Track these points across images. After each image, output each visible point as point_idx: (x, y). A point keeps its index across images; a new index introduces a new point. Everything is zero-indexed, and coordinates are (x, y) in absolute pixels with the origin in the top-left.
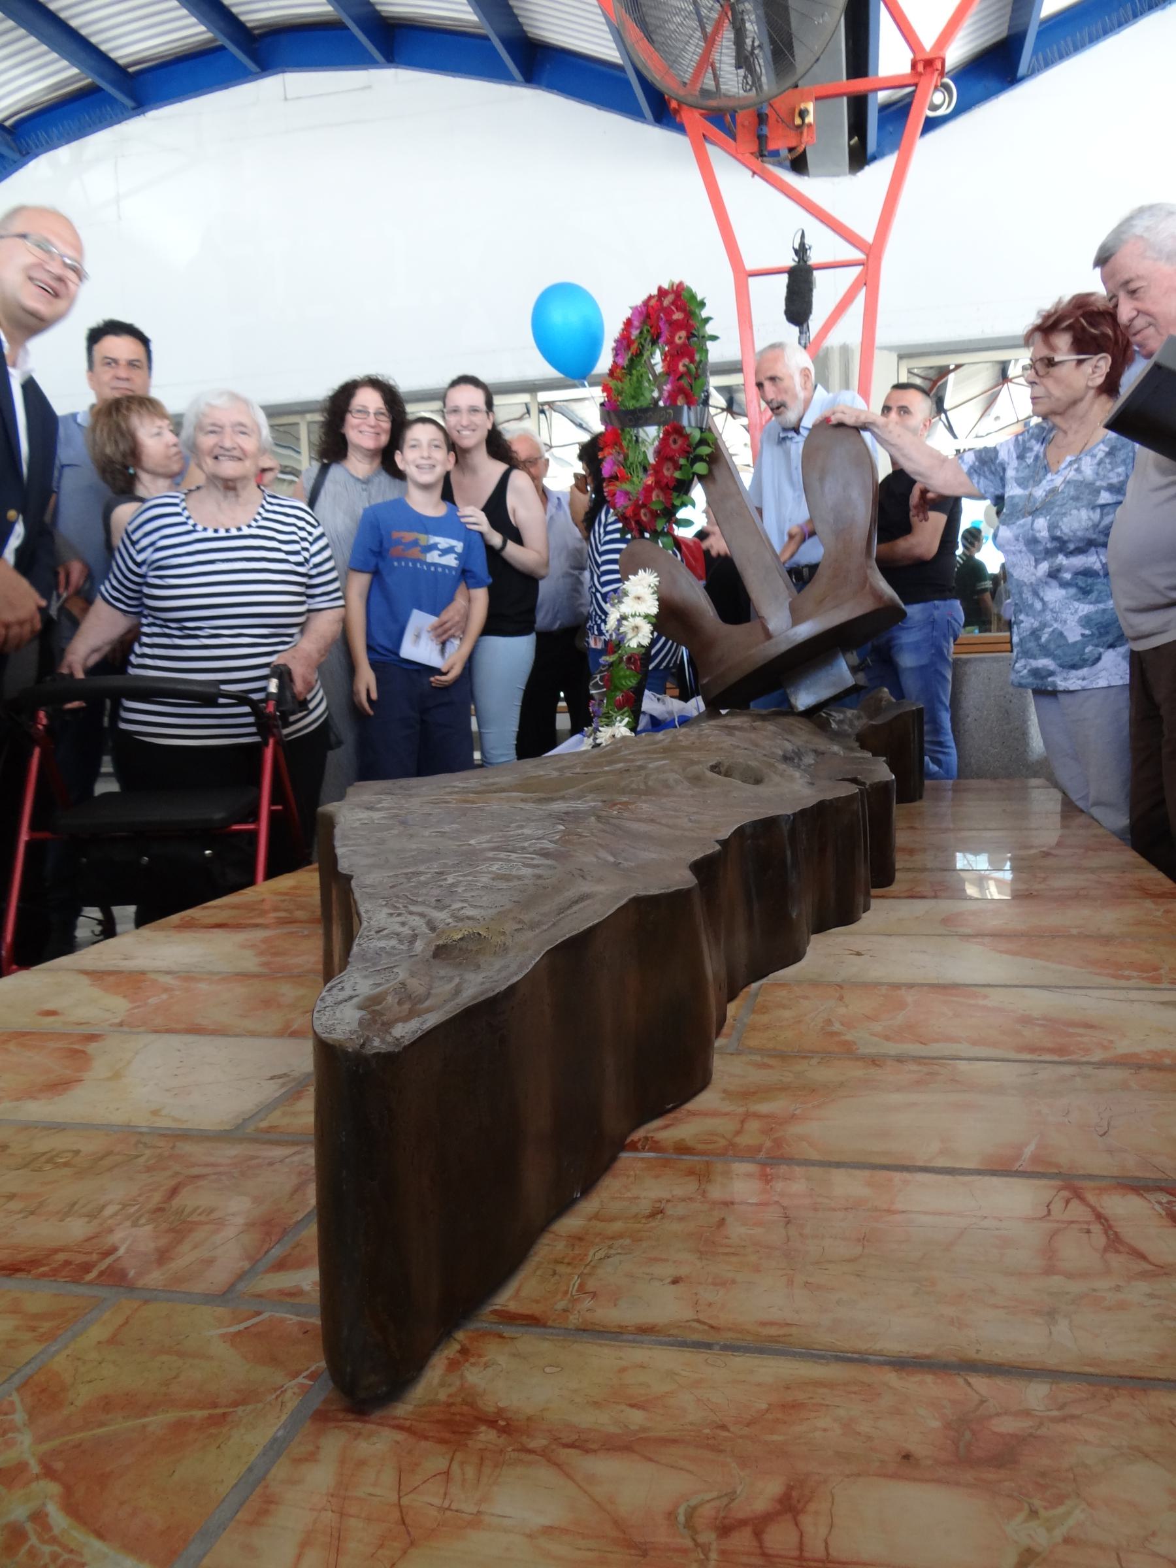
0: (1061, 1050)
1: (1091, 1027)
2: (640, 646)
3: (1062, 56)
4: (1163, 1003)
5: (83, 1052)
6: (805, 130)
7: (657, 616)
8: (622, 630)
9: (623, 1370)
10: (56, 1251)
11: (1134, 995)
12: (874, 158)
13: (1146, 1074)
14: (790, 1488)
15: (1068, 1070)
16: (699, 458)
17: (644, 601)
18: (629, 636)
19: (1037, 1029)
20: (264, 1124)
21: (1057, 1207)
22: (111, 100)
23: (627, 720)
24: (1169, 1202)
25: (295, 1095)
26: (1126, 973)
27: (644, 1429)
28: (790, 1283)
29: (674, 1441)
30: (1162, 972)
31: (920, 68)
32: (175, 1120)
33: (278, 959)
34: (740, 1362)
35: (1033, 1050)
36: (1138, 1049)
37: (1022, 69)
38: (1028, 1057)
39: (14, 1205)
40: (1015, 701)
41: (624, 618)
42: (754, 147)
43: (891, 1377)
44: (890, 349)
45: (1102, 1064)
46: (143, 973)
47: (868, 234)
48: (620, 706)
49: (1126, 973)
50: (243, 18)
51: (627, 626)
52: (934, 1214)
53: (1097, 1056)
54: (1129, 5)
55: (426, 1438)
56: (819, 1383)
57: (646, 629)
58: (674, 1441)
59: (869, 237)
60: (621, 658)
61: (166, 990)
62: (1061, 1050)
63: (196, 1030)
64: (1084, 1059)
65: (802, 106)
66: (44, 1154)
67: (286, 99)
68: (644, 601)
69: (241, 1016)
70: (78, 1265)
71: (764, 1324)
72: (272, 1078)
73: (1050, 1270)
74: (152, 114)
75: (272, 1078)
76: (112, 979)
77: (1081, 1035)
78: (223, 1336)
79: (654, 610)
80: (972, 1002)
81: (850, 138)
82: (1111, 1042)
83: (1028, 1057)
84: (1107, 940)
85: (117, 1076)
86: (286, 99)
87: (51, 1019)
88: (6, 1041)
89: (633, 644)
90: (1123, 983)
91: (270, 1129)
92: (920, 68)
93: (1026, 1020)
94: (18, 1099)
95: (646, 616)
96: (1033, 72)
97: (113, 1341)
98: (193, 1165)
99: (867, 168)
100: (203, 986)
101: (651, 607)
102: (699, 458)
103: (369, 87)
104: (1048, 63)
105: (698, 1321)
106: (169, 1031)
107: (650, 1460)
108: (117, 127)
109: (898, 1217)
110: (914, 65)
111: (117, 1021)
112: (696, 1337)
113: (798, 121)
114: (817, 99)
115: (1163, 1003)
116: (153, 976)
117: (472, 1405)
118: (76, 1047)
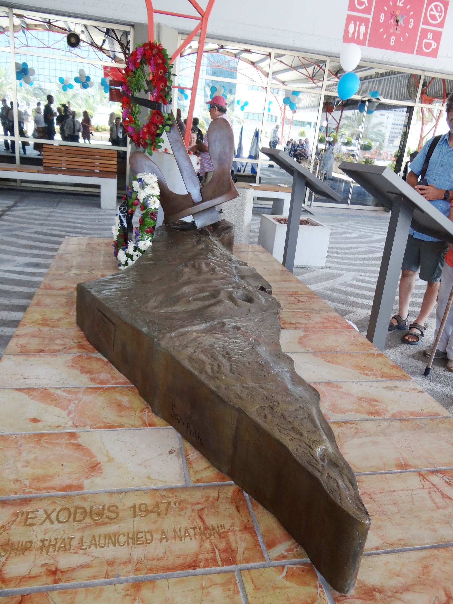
1: (377, 401)
2: (155, 209)
4: (386, 388)
5: (79, 445)
7: (159, 195)
8: (149, 202)
9: (385, 565)
10: (197, 555)
11: (377, 384)
13: (404, 423)
14: (445, 592)
15: (386, 423)
16: (168, 125)
17: (155, 189)
18: (151, 204)
19: (366, 403)
20: (194, 480)
21: (423, 482)
23: (150, 238)
24: (443, 477)
25: (189, 463)
27: (406, 583)
28: (392, 523)
29: (415, 585)
30: (375, 371)
32: (161, 481)
33: (93, 376)
34: (406, 554)
35: (371, 414)
36: (395, 411)
38: (372, 417)
39: (157, 536)
40: (241, 206)
41: (148, 197)
43: (435, 552)
46: (46, 389)
48: (147, 232)
51: (150, 201)
52: (402, 490)
53: (388, 416)
55: (367, 600)
56: (426, 558)
57: (158, 202)
58: (415, 585)
60: (147, 213)
61: (69, 400)
62: (377, 413)
63: (110, 426)
66: (134, 507)
68: (155, 189)
69: (121, 416)
70: (211, 559)
71: (399, 540)
72: (170, 453)
73: (438, 508)
75: (170, 453)
76: (35, 393)
78: (283, 578)
79: (158, 193)
80: (340, 390)
85: (111, 459)
87: (40, 425)
88: (38, 442)
89: (153, 208)
91: (198, 481)
93: (360, 399)
94: (87, 478)
95: (157, 196)
97: (257, 588)
98: (193, 505)
100: (80, 396)
101: (157, 191)
102: (168, 125)
105: (385, 543)
106: (100, 427)
107: (414, 592)
109: (395, 493)
111: (71, 423)
112: (389, 549)
115: (386, 388)
116: (52, 391)
117: (365, 586)
118: (72, 442)
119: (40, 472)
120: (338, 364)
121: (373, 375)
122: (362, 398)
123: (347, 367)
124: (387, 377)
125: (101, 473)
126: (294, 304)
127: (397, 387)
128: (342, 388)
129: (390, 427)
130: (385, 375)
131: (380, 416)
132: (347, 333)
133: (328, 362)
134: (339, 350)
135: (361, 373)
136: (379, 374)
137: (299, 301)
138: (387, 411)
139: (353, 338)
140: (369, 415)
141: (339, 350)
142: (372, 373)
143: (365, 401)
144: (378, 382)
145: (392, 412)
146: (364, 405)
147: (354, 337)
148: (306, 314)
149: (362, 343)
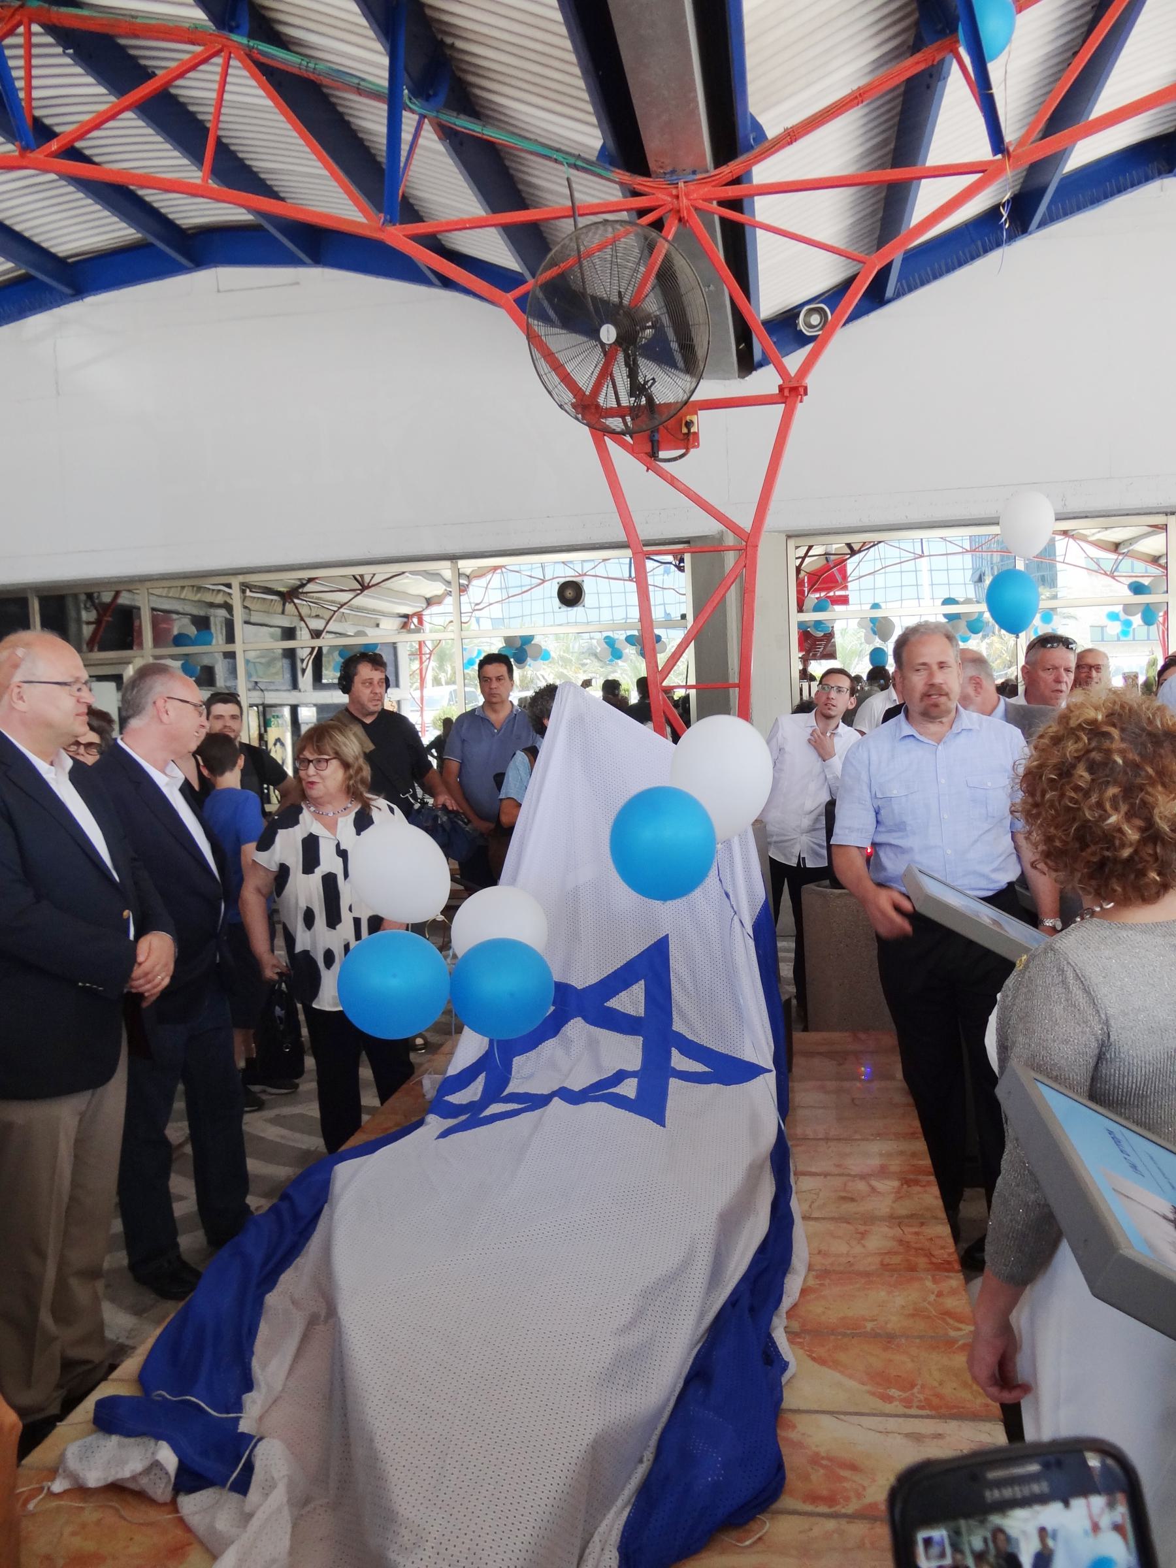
0: (831, 1500)
1: (853, 1467)
3: (924, 283)
4: (907, 1435)
6: (691, 438)
11: (892, 1424)
12: (761, 365)
15: (831, 1524)
19: (822, 1471)
22: (50, 289)
26: (893, 1392)
30: (915, 1390)
31: (786, 393)
37: (889, 292)
38: (809, 1508)
42: (649, 450)
44: (780, 532)
45: (852, 1517)
47: (746, 523)
49: (893, 1392)
50: (178, 222)
53: (850, 1509)
54: (979, 243)
59: (746, 523)
62: (831, 1500)
64: (843, 1511)
65: (688, 418)
67: (219, 291)
74: (90, 300)
77: (845, 1479)
81: (738, 344)
82: (864, 1488)
83: (809, 1508)
84: (887, 1339)
86: (219, 291)
90: (888, 1408)
92: (786, 393)
96: (898, 295)
99: (754, 373)
103: (298, 283)
104: (911, 289)
108: (56, 311)
110: (781, 388)
113: (685, 430)
114: (692, 553)
115: (907, 1435)
119: (90, 1546)
120: (835, 1365)
121: (901, 1400)
122: (823, 1458)
123: (851, 1377)
124: (932, 1407)
125: (181, 1563)
126: (852, 1200)
127: (939, 1436)
128: (794, 1427)
129: (835, 1535)
130: (935, 1401)
131: (830, 1507)
132: (929, 1284)
133: (814, 1359)
134: (868, 1329)
135: (873, 1394)
136: (921, 1397)
137: (873, 1190)
138: (859, 1496)
139: (932, 1298)
140: (804, 1502)
141: (868, 1329)
142: (904, 1395)
143: (822, 1466)
144: (901, 1420)
145: (868, 1500)
146: (814, 1477)
147: (940, 1294)
148: (862, 1228)
149: (948, 1313)
